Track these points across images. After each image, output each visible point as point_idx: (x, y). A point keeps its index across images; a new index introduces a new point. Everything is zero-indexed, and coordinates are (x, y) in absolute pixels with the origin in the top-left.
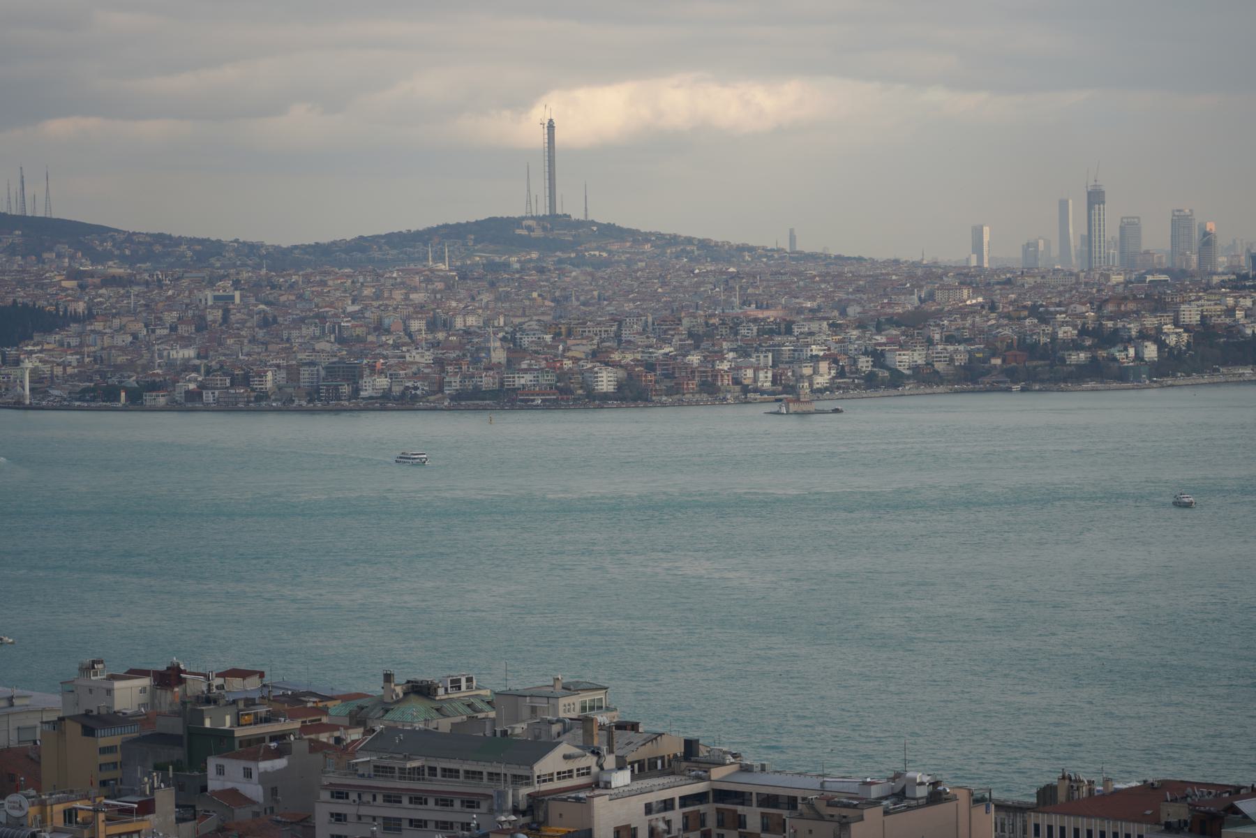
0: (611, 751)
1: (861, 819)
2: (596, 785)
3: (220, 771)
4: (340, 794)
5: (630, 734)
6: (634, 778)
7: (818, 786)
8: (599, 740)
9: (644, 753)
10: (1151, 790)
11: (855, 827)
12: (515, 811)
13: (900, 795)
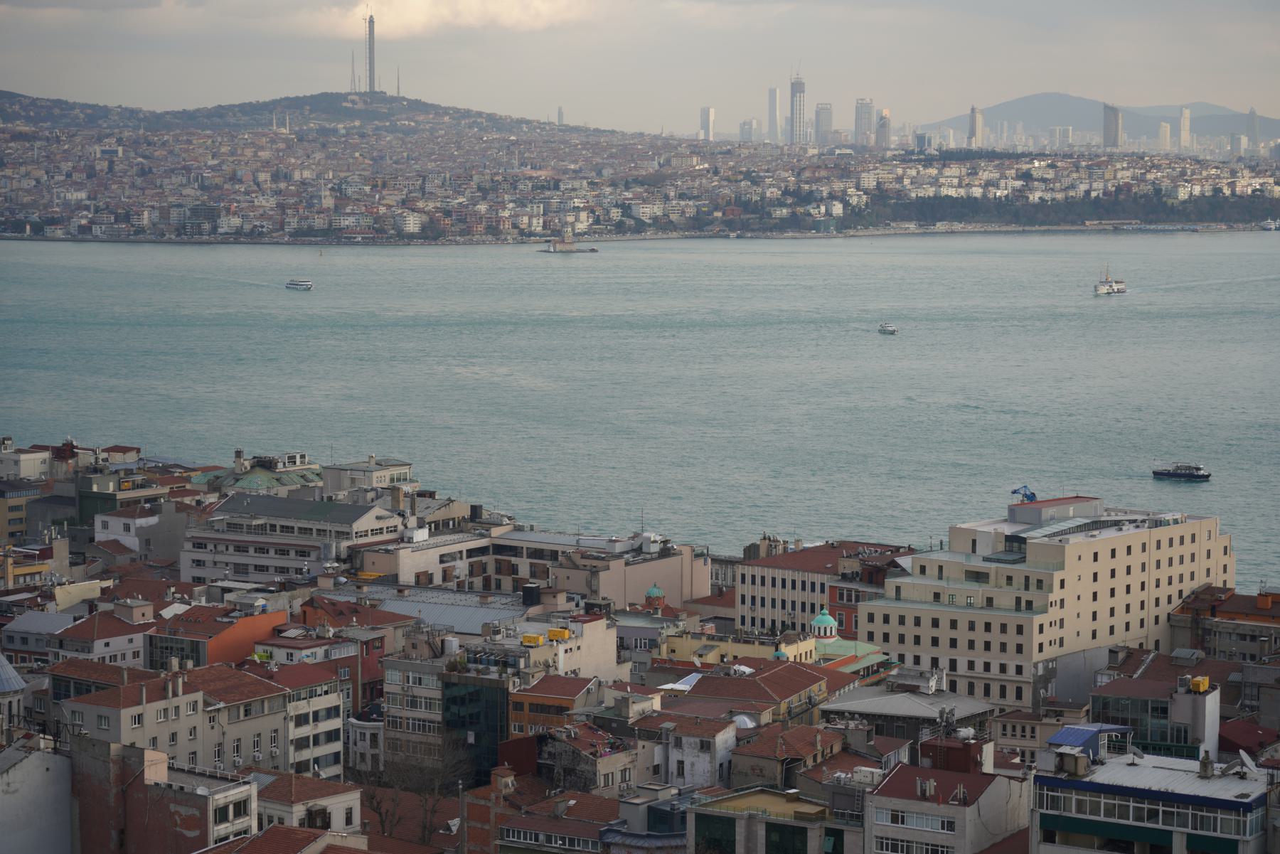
0: (413, 514)
1: (608, 568)
2: (401, 540)
3: (105, 525)
4: (199, 545)
6: (431, 535)
7: (574, 543)
8: (404, 505)
9: (440, 515)
10: (833, 550)
11: (602, 575)
12: (338, 559)
13: (638, 550)
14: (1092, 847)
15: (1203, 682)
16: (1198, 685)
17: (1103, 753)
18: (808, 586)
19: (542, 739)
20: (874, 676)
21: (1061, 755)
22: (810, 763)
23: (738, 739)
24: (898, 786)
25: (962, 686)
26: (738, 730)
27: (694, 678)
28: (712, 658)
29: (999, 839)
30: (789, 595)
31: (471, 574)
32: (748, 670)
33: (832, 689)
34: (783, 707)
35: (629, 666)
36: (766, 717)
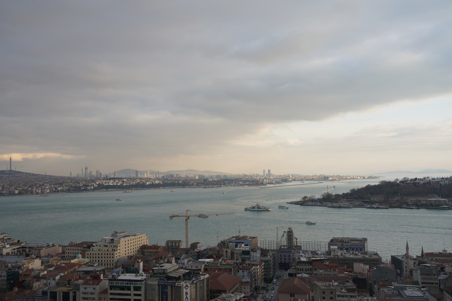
0: (6, 242)
1: (42, 249)
5: (10, 240)
6: (10, 246)
7: (37, 245)
9: (12, 242)
10: (82, 243)
13: (48, 246)
15: (140, 261)
16: (139, 261)
17: (120, 274)
18: (78, 250)
19: (23, 281)
20: (87, 264)
21: (113, 275)
22: (73, 280)
23: (60, 277)
25: (100, 265)
26: (60, 276)
27: (54, 267)
28: (59, 263)
29: (103, 290)
30: (75, 251)
31: (17, 252)
32: (64, 265)
33: (79, 267)
34: (70, 271)
35: (43, 266)
36: (66, 273)
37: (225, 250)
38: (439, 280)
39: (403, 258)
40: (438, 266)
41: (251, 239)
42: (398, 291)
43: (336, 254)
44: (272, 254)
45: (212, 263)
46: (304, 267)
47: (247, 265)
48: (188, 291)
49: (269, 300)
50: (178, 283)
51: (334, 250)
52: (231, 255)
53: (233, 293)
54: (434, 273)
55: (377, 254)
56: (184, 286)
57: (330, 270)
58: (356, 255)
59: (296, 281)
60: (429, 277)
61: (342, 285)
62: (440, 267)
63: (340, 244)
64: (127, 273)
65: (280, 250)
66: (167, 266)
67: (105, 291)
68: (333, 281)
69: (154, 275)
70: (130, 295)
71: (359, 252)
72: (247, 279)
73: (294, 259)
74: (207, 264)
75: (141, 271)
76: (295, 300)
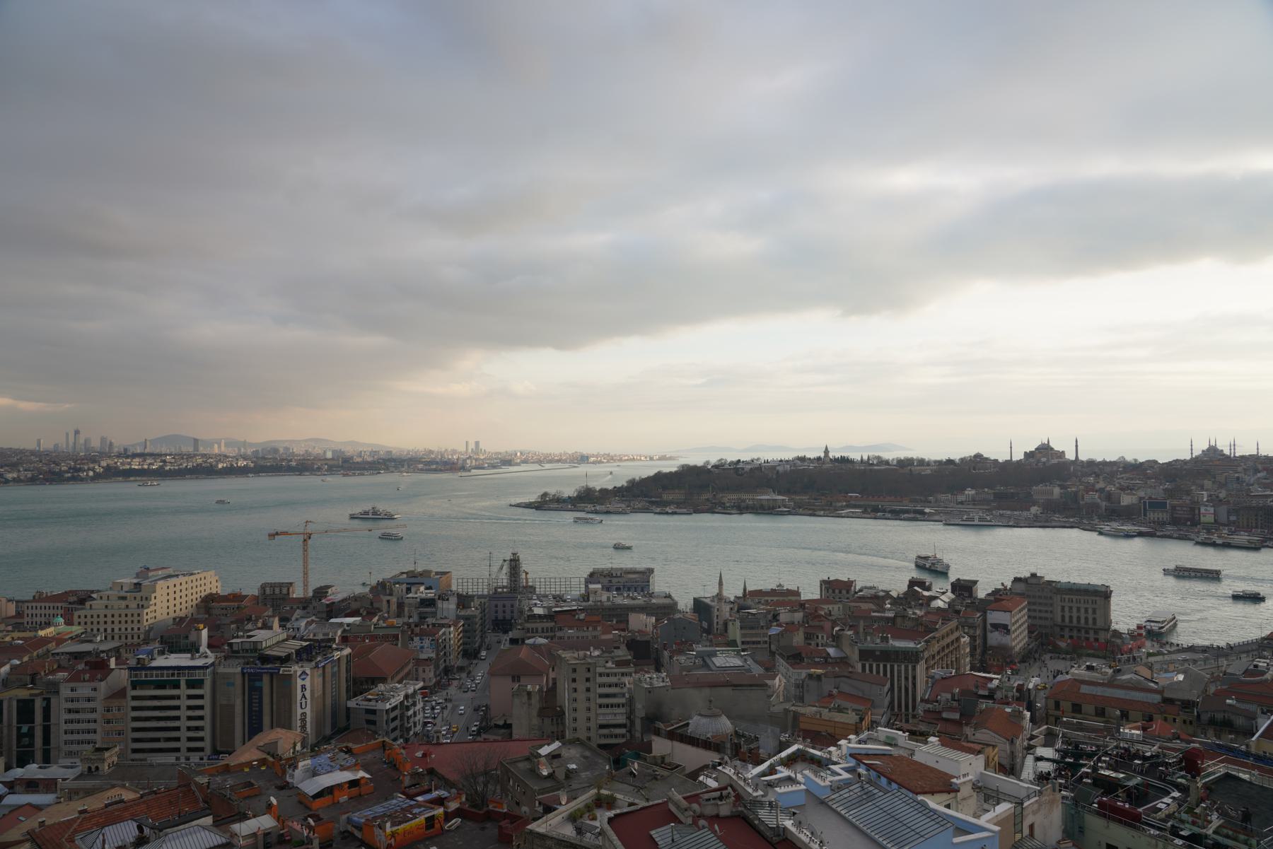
14: (150, 689)
15: (201, 626)
17: (156, 656)
18: (56, 608)
20: (76, 639)
22: (43, 673)
24: (76, 678)
25: (109, 638)
26: (11, 665)
29: (116, 691)
30: (47, 612)
32: (21, 642)
33: (58, 645)
34: (35, 654)
36: (26, 659)
37: (385, 598)
38: (770, 636)
39: (713, 601)
40: (769, 612)
41: (438, 576)
42: (704, 660)
43: (599, 599)
44: (479, 603)
45: (358, 626)
46: (539, 625)
47: (430, 627)
48: (307, 683)
49: (473, 691)
50: (285, 669)
51: (596, 592)
52: (398, 607)
53: (399, 682)
54: (762, 624)
55: (669, 596)
56: (299, 673)
57: (588, 628)
58: (633, 599)
59: (524, 653)
60: (754, 632)
61: (606, 655)
62: (772, 613)
63: (605, 581)
64: (172, 652)
65: (495, 596)
66: (261, 635)
67: (121, 693)
68: (592, 649)
69: (233, 654)
70: (178, 697)
71: (639, 594)
72: (429, 653)
73: (521, 612)
74: (347, 628)
75: (204, 648)
76: (521, 687)
